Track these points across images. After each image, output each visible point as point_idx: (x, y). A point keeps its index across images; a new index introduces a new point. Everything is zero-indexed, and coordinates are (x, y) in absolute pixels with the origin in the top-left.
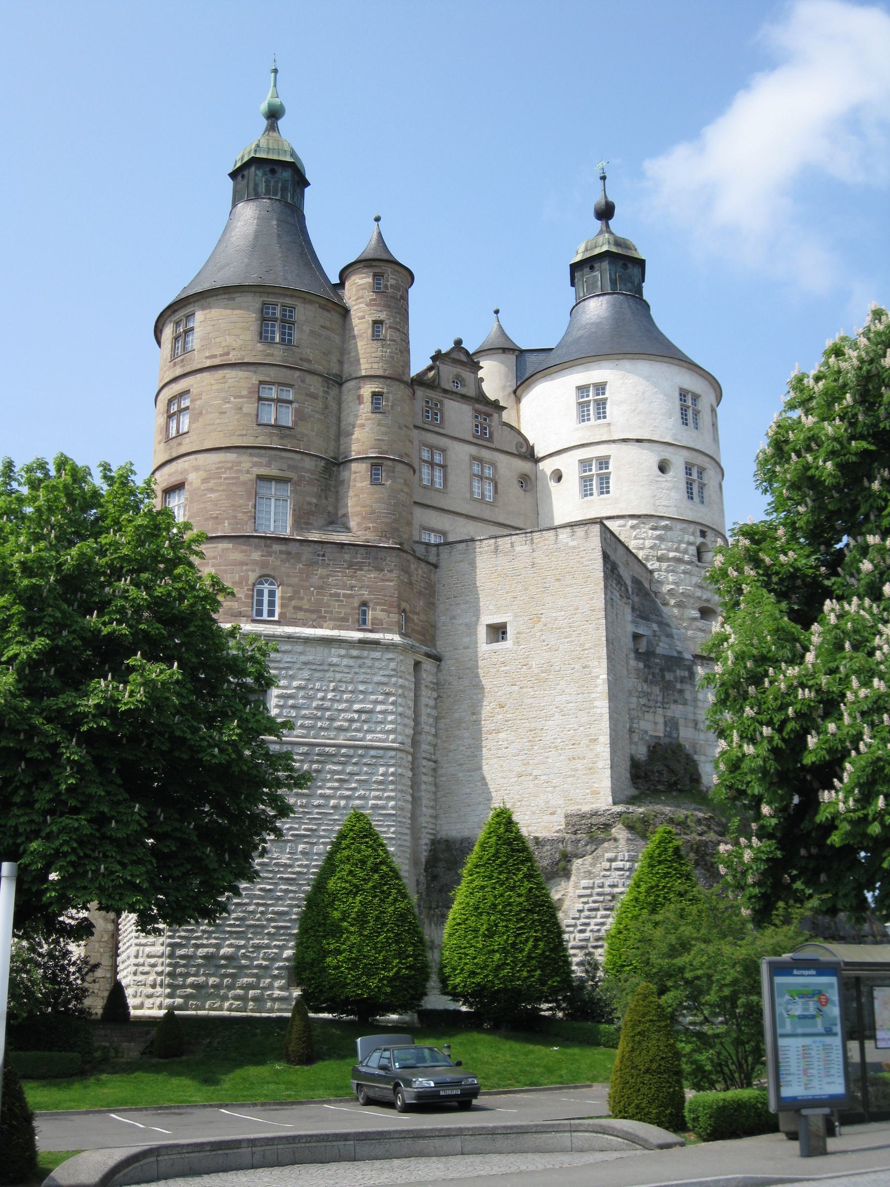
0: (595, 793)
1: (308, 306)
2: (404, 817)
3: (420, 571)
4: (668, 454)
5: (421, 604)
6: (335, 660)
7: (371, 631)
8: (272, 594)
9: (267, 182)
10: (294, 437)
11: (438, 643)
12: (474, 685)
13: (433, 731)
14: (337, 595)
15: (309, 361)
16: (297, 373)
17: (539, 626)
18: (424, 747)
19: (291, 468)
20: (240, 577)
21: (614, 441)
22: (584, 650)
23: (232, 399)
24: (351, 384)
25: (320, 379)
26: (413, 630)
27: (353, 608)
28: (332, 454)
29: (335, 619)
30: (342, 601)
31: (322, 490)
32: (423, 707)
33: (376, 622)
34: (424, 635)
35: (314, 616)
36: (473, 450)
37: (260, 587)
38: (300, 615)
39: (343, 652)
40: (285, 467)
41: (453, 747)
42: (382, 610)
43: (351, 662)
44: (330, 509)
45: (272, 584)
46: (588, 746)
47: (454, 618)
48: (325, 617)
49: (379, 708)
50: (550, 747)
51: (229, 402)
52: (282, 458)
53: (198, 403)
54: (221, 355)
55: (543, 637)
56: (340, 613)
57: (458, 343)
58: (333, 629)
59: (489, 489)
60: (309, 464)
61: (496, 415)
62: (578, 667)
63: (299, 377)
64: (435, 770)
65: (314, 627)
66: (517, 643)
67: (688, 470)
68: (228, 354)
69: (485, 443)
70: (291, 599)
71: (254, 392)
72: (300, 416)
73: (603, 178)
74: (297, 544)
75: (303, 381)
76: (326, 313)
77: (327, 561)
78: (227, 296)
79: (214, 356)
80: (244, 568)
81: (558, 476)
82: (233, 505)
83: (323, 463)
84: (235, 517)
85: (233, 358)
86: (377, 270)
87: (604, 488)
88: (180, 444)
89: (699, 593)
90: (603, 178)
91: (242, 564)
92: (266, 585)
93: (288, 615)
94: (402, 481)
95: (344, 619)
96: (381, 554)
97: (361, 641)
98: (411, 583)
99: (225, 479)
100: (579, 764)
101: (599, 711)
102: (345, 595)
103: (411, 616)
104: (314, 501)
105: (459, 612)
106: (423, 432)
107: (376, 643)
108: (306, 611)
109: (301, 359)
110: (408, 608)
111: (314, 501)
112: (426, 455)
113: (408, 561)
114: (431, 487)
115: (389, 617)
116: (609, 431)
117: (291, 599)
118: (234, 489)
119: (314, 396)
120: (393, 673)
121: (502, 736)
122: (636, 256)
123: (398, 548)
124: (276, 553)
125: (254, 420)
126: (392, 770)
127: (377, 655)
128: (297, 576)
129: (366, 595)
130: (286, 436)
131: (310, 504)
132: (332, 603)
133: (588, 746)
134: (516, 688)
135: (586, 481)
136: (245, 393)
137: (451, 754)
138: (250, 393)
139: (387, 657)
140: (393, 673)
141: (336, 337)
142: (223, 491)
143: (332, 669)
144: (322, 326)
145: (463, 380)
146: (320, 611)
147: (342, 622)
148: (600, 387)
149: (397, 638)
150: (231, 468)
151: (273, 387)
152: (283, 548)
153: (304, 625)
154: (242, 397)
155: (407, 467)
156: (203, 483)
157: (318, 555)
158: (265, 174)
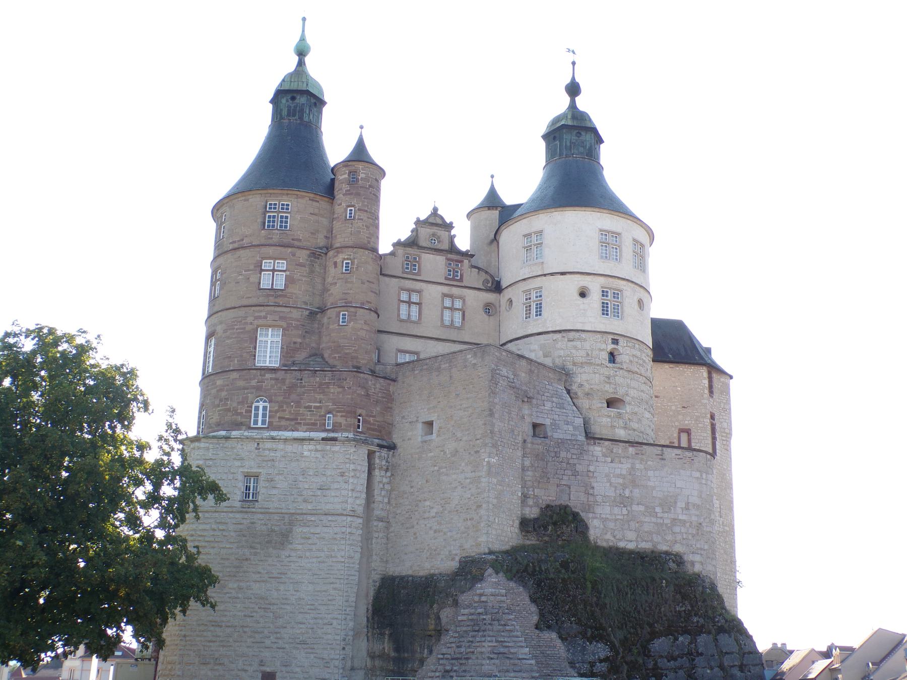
0: (478, 545)
1: (300, 200)
2: (353, 563)
3: (378, 386)
4: (586, 281)
5: (378, 409)
6: (306, 453)
7: (333, 431)
8: (265, 408)
9: (289, 107)
10: (285, 296)
11: (394, 436)
12: (413, 467)
13: (386, 500)
14: (310, 407)
15: (300, 240)
16: (290, 250)
17: (452, 423)
18: (377, 512)
19: (282, 318)
20: (243, 397)
21: (545, 275)
22: (476, 440)
24: (331, 253)
25: (308, 252)
26: (369, 429)
27: (320, 416)
28: (317, 306)
29: (308, 424)
30: (313, 411)
31: (306, 332)
32: (377, 484)
33: (337, 425)
34: (380, 432)
35: (293, 423)
36: (446, 290)
37: (257, 404)
38: (283, 423)
39: (311, 447)
40: (277, 318)
41: (398, 512)
42: (342, 416)
43: (319, 455)
44: (314, 345)
45: (265, 401)
46: (475, 510)
47: (403, 417)
48: (301, 423)
49: (336, 486)
50: (454, 511)
52: (276, 312)
53: (224, 276)
54: (238, 241)
55: (454, 431)
56: (310, 419)
57: (435, 210)
58: (306, 431)
59: (458, 316)
60: (296, 314)
61: (466, 262)
62: (472, 453)
63: (291, 252)
64: (387, 528)
65: (293, 431)
66: (438, 436)
67: (604, 294)
68: (243, 240)
69: (455, 283)
70: (277, 412)
71: (258, 266)
72: (290, 280)
73: (574, 63)
74: (284, 372)
75: (294, 255)
76: (315, 204)
77: (304, 384)
78: (243, 198)
79: (234, 242)
80: (246, 391)
82: (240, 348)
83: (307, 313)
84: (241, 356)
85: (246, 242)
86: (353, 168)
87: (539, 313)
89: (607, 387)
90: (574, 63)
91: (245, 388)
92: (261, 403)
93: (274, 423)
94: (363, 322)
95: (314, 424)
96: (344, 375)
97: (323, 439)
98: (368, 395)
100: (469, 523)
101: (483, 484)
102: (316, 407)
103: (367, 418)
104: (299, 340)
105: (407, 413)
106: (402, 280)
107: (334, 439)
108: (288, 419)
109: (293, 240)
110: (364, 412)
111: (299, 340)
112: (404, 296)
113: (366, 379)
114: (408, 320)
115: (346, 421)
116: (543, 268)
117: (277, 412)
118: (242, 336)
119: (302, 265)
120: (347, 461)
121: (427, 503)
122: (587, 126)
123: (355, 371)
124: (267, 379)
125: (257, 287)
126: (344, 529)
127: (336, 448)
128: (282, 395)
129: (331, 406)
130: (280, 296)
131: (295, 343)
132: (306, 413)
133: (475, 510)
134: (436, 468)
136: (252, 267)
137: (397, 516)
138: (255, 267)
139: (344, 449)
140: (347, 461)
141: (324, 219)
142: (235, 338)
143: (303, 459)
144: (311, 214)
145: (439, 238)
146: (297, 419)
147: (313, 427)
148: (540, 233)
149: (351, 435)
150: (241, 322)
151: (272, 261)
152: (273, 376)
153: (286, 429)
154: (249, 270)
155: (368, 311)
156: (224, 333)
157: (298, 380)
158: (287, 101)
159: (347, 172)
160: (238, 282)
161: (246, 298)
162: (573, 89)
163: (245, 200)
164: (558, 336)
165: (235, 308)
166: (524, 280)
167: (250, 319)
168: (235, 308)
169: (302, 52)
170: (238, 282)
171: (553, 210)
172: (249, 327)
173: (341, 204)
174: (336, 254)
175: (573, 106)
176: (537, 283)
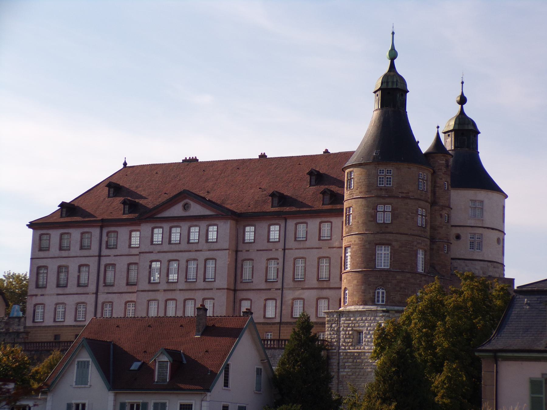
21: (484, 228)
23: (410, 214)
51: (409, 215)
54: (406, 193)
68: (408, 193)
73: (462, 83)
80: (415, 286)
81: (458, 237)
88: (387, 227)
90: (462, 83)
99: (409, 248)
135: (472, 243)
159: (445, 159)
160: (408, 219)
161: (413, 230)
162: (463, 100)
163: (409, 168)
164: (489, 264)
165: (406, 234)
166: (472, 227)
167: (415, 243)
168: (406, 234)
169: (393, 55)
170: (408, 219)
171: (490, 191)
172: (415, 248)
173: (441, 179)
174: (441, 209)
175: (462, 112)
176: (480, 231)
